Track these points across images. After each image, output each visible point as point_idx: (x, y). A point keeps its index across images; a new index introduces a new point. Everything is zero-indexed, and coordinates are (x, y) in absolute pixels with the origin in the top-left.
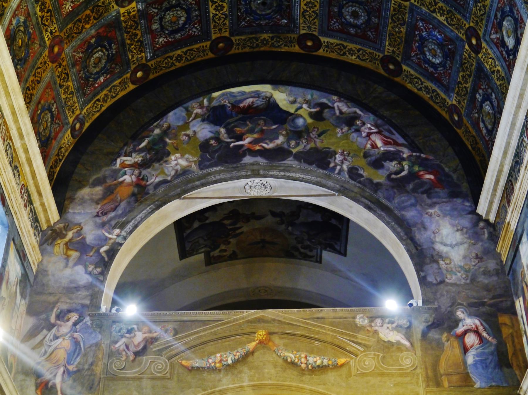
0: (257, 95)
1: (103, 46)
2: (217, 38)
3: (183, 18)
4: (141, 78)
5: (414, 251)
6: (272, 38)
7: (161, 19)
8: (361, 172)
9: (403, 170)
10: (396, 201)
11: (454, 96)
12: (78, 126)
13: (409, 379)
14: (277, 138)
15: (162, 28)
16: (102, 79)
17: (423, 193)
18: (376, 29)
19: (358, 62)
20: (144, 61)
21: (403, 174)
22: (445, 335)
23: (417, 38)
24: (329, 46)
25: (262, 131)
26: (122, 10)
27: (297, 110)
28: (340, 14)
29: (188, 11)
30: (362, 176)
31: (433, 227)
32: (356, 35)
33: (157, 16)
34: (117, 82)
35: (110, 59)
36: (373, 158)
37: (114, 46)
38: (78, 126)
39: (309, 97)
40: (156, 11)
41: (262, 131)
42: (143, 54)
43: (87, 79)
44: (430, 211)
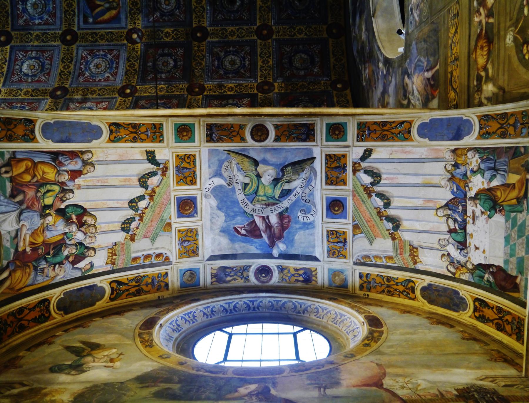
3: (303, 55)
7: (297, 69)
20: (329, 82)
26: (276, 90)
33: (293, 71)
34: (335, 99)
40: (289, 72)
42: (322, 82)
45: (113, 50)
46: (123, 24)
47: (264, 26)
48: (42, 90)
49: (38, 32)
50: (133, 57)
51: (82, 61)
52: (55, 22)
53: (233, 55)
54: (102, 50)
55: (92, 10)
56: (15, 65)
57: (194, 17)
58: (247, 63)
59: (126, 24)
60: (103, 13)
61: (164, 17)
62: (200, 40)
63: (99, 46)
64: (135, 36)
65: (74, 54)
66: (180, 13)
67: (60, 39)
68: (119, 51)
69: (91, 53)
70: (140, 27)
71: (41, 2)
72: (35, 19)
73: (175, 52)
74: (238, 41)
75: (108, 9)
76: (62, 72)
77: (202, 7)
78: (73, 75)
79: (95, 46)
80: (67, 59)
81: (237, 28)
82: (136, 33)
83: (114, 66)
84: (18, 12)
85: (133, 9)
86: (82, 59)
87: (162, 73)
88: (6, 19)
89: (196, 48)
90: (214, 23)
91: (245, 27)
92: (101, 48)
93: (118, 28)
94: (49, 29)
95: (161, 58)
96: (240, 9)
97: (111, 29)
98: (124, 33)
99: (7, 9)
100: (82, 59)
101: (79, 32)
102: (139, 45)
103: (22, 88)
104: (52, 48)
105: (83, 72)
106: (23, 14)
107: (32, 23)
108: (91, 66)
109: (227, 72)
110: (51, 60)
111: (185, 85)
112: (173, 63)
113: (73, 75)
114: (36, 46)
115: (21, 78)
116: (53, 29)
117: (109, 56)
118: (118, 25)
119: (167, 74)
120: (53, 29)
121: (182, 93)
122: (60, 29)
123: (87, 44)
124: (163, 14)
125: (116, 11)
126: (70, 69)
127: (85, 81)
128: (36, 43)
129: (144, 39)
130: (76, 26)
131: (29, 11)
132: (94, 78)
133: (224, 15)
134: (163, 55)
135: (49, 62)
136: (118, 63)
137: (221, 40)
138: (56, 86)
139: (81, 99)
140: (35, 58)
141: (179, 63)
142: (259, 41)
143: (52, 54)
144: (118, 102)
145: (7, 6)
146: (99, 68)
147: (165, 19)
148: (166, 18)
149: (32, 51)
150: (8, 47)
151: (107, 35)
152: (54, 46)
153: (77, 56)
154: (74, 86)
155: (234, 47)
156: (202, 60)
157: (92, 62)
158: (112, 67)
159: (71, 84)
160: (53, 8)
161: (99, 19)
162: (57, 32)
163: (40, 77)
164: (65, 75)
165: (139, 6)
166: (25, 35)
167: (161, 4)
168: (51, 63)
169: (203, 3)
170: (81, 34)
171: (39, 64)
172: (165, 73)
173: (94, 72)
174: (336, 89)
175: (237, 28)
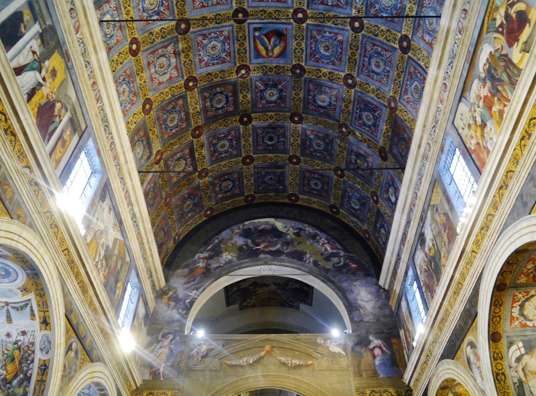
0: (267, 223)
1: (191, 199)
2: (248, 195)
3: (231, 185)
4: (209, 214)
5: (347, 304)
6: (275, 195)
7: (220, 186)
8: (320, 263)
9: (341, 262)
10: (338, 278)
11: (366, 225)
12: (177, 238)
13: (345, 373)
14: (277, 245)
15: (221, 190)
16: (190, 215)
17: (351, 274)
18: (327, 192)
19: (318, 207)
20: (211, 206)
21: (341, 264)
22: (364, 349)
23: (347, 196)
24: (303, 199)
25: (269, 242)
26: (201, 181)
27: (287, 231)
28: (309, 184)
29: (233, 182)
30: (320, 265)
31: (357, 292)
32: (317, 194)
34: (197, 216)
35: (195, 205)
36: (326, 256)
37: (196, 199)
38: (177, 238)
39: (293, 225)
41: (269, 242)
43: (182, 215)
44: (355, 283)
46: (254, 61)
47: (252, 160)
48: (184, 9)
51: (218, 33)
53: (230, 145)
54: (230, 48)
55: (267, 35)
58: (223, 155)
59: (254, 63)
60: (263, 44)
62: (241, 121)
63: (234, 43)
64: (243, 72)
67: (239, 8)
68: (229, 62)
69: (227, 38)
70: (251, 75)
74: (240, 146)
75: (266, 49)
77: (267, 120)
78: (203, 30)
79: (233, 40)
80: (218, 19)
82: (246, 72)
83: (215, 62)
85: (266, 68)
86: (219, 32)
87: (211, 101)
89: (234, 119)
90: (254, 128)
91: (251, 148)
92: (232, 45)
93: (250, 57)
95: (224, 96)
97: (250, 52)
100: (219, 32)
101: (246, 24)
102: (236, 77)
108: (214, 42)
109: (214, 145)
111: (201, 122)
113: (203, 30)
117: (225, 54)
119: (210, 106)
121: (193, 125)
122: (248, 7)
123: (235, 33)
124: (262, 91)
126: (209, 24)
127: (198, 43)
129: (241, 79)
134: (227, 97)
136: (218, 63)
139: (179, 51)
142: (241, 158)
143: (224, 4)
144: (179, 83)
146: (212, 49)
148: (258, 94)
152: (231, 4)
154: (192, 36)
155: (236, 144)
156: (225, 125)
158: (213, 60)
159: (194, 32)
162: (245, 4)
165: (269, 73)
167: (270, 90)
168: (215, 5)
174: (207, 211)
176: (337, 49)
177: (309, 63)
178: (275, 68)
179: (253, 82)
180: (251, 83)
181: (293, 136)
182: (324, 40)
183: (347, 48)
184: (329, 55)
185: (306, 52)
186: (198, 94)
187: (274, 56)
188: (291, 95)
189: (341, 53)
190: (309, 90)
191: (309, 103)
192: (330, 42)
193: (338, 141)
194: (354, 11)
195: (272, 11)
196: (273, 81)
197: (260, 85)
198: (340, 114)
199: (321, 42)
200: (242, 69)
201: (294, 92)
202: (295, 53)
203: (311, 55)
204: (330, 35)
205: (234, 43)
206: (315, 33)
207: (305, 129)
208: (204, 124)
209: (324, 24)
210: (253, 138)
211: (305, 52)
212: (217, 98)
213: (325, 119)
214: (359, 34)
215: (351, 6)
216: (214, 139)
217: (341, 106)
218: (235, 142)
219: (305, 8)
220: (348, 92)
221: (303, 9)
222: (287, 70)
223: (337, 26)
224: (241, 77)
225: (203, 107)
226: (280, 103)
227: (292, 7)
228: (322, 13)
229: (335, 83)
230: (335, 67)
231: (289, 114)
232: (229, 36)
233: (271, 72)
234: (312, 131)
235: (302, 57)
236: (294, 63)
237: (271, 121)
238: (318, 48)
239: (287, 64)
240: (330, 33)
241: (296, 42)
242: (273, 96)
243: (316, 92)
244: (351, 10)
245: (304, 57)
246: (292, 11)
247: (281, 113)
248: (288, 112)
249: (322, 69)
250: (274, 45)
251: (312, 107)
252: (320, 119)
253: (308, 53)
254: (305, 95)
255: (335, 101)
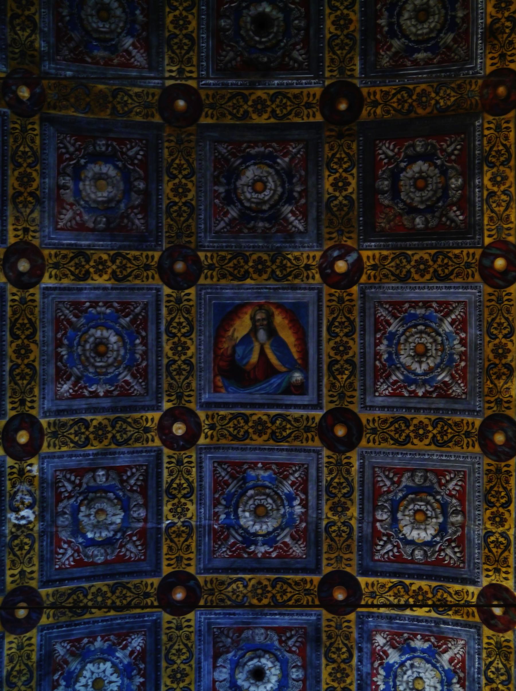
45: (376, 320)
46: (310, 296)
48: (490, 481)
49: (325, 508)
50: (397, 266)
51: (406, 394)
52: (301, 465)
53: (400, 14)
54: (376, 345)
55: (271, 371)
56: (412, 562)
57: (299, 120)
61: (296, 194)
63: (363, 355)
64: (341, 266)
65: (384, 414)
66: (285, 155)
67: (344, 453)
68: (381, 304)
70: (319, 254)
71: (252, 497)
72: (291, 514)
73: (389, 163)
75: (272, 332)
76: (434, 441)
77: (273, 98)
78: (446, 411)
79: (364, 364)
81: (327, 11)
82: (332, 265)
83: (420, 312)
84: (274, 555)
85: (273, 272)
87: (446, 188)
88: (290, 585)
89: (379, 111)
92: (370, 352)
93: (320, 309)
94: (319, 480)
95: (403, 196)
96: (281, 5)
97: (320, 325)
98: (331, 295)
99: (265, 583)
100: (401, 396)
101: (327, 406)
102: (365, 254)
103: (482, 533)
104: (368, 473)
105: (436, 388)
106: (279, 544)
107: (301, 521)
108: (419, 371)
110: (400, 472)
112: (420, 163)
113: (446, 411)
114: (362, 511)
115: (450, 541)
116: (319, 470)
117: (391, 329)
118: (312, 310)
120: (319, 470)
122: (318, 453)
123: (357, 385)
124: (290, 199)
125: (276, 312)
128: (354, 511)
129: (349, 243)
130: (312, 413)
131: (271, 529)
132: (456, 357)
133: (295, 45)
135: (407, 475)
136: (414, 304)
137: (358, 50)
138: (477, 449)
140: (393, 512)
141: (418, 149)
143: (384, 469)
145: (259, 583)
146: (427, 350)
147: (300, 193)
148: (298, 189)
149: (375, 520)
150: (362, 580)
151: (337, 335)
152: (362, 466)
153: (390, 408)
156: (410, 93)
157: (408, 369)
159: (472, 412)
160: (266, 470)
161: (296, 356)
162: (325, 460)
163: (451, 495)
164: (443, 433)
165: (265, 257)
166: (332, 540)
167: (264, 202)
168: (408, 470)
169: (264, 97)
170: (332, 402)
171: (413, 501)
172: (448, 179)
173: (438, 360)
175: (327, 11)
176: (70, 354)
177: (148, 298)
178: (247, 272)
179: (312, 228)
180: (318, 229)
181: (188, 36)
182: (111, 370)
183: (43, 363)
184: (92, 331)
185: (158, 328)
186: (481, 225)
187: (250, 311)
188: (198, 187)
189: (59, 344)
190: (144, 208)
191: (143, 165)
192: (91, 370)
193: (40, 44)
194: (35, 470)
195: (255, 437)
196: (253, 229)
197: (292, 218)
198: (43, 148)
199: (117, 363)
200: (344, 275)
201: (190, 196)
202: (190, 323)
203: (145, 319)
204: (93, 388)
205: (363, 355)
206: (137, 388)
207: (150, 69)
208: (476, 117)
209: (112, 416)
210: (320, 31)
211: (163, 327)
212: (426, 194)
213: (92, 116)
214: (13, 413)
215: (42, 480)
216: (448, 48)
217: (43, 176)
218: (383, 22)
219: (166, 451)
220: (26, 231)
221: (171, 448)
222: (211, 267)
223: (76, 417)
224: (349, 250)
225: (472, 177)
226: (234, 155)
227: (200, 450)
228: (119, 444)
229: (69, 247)
230: (72, 297)
231: (204, 120)
232: (376, 379)
233: (260, 260)
234: (127, 65)
235: (170, 312)
236: (192, 290)
237: (259, 93)
238: (124, 344)
239: (211, 286)
240: (95, 395)
241: (189, 353)
242: (255, 182)
243: (122, 206)
244: (41, 470)
245: (164, 311)
246: (202, 441)
247: (228, 120)
248: (208, 126)
249: (109, 284)
250: (251, 342)
251: (131, 153)
252: (105, 115)
253: (152, 327)
254: (158, 190)
255: (65, 187)
